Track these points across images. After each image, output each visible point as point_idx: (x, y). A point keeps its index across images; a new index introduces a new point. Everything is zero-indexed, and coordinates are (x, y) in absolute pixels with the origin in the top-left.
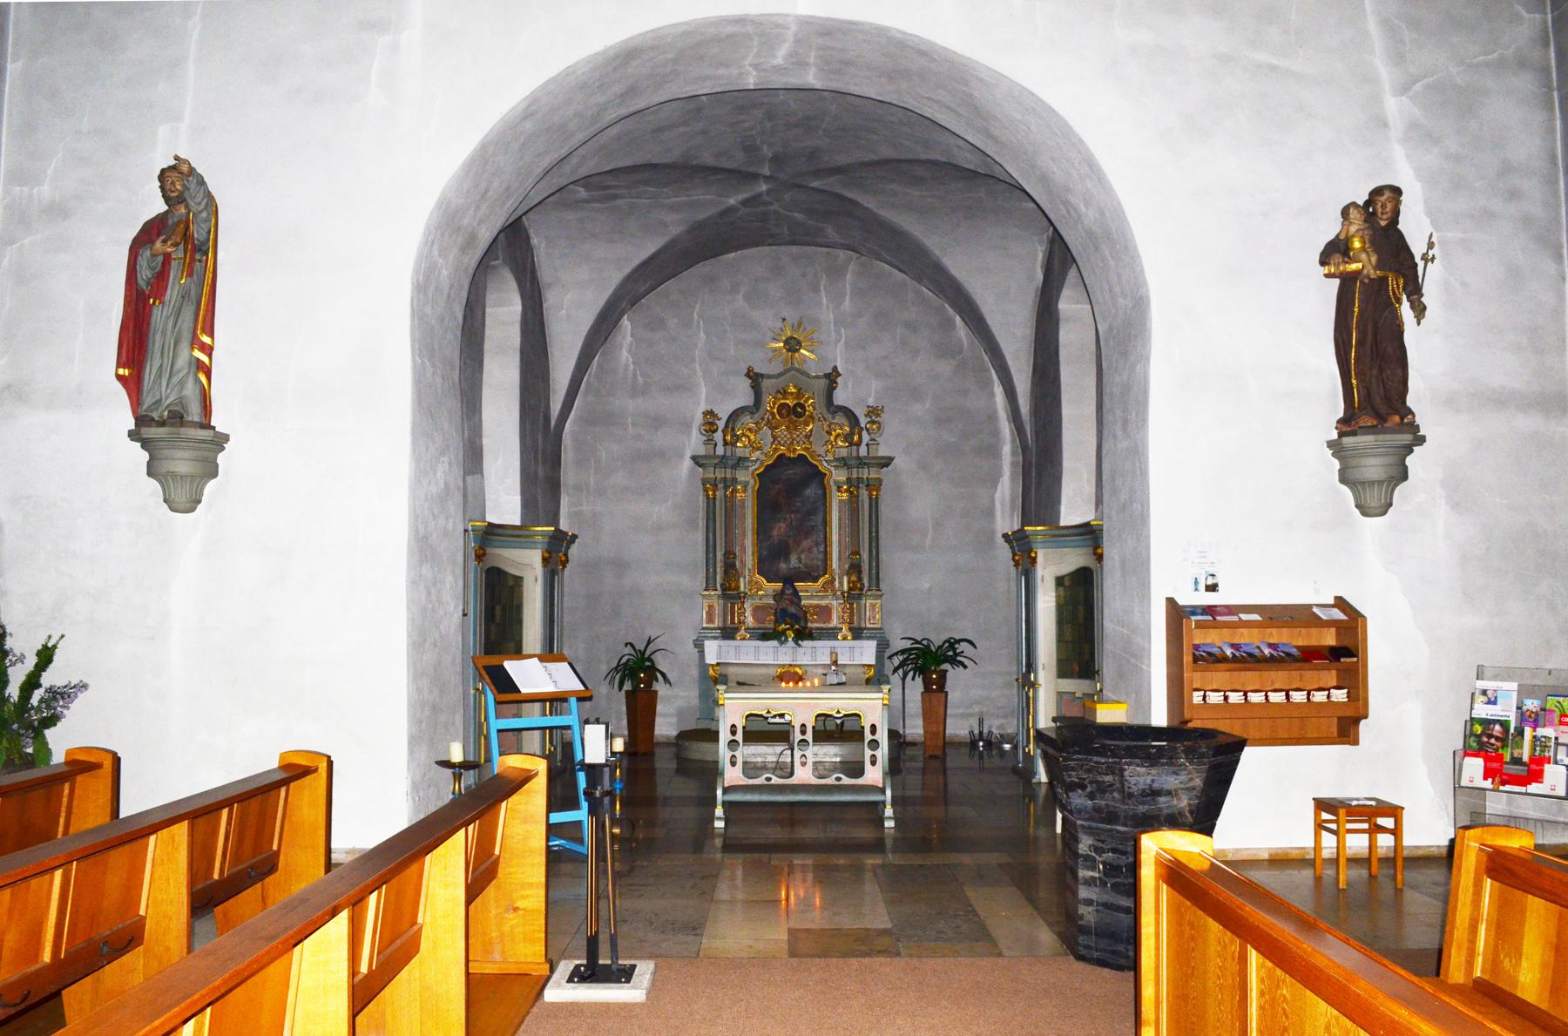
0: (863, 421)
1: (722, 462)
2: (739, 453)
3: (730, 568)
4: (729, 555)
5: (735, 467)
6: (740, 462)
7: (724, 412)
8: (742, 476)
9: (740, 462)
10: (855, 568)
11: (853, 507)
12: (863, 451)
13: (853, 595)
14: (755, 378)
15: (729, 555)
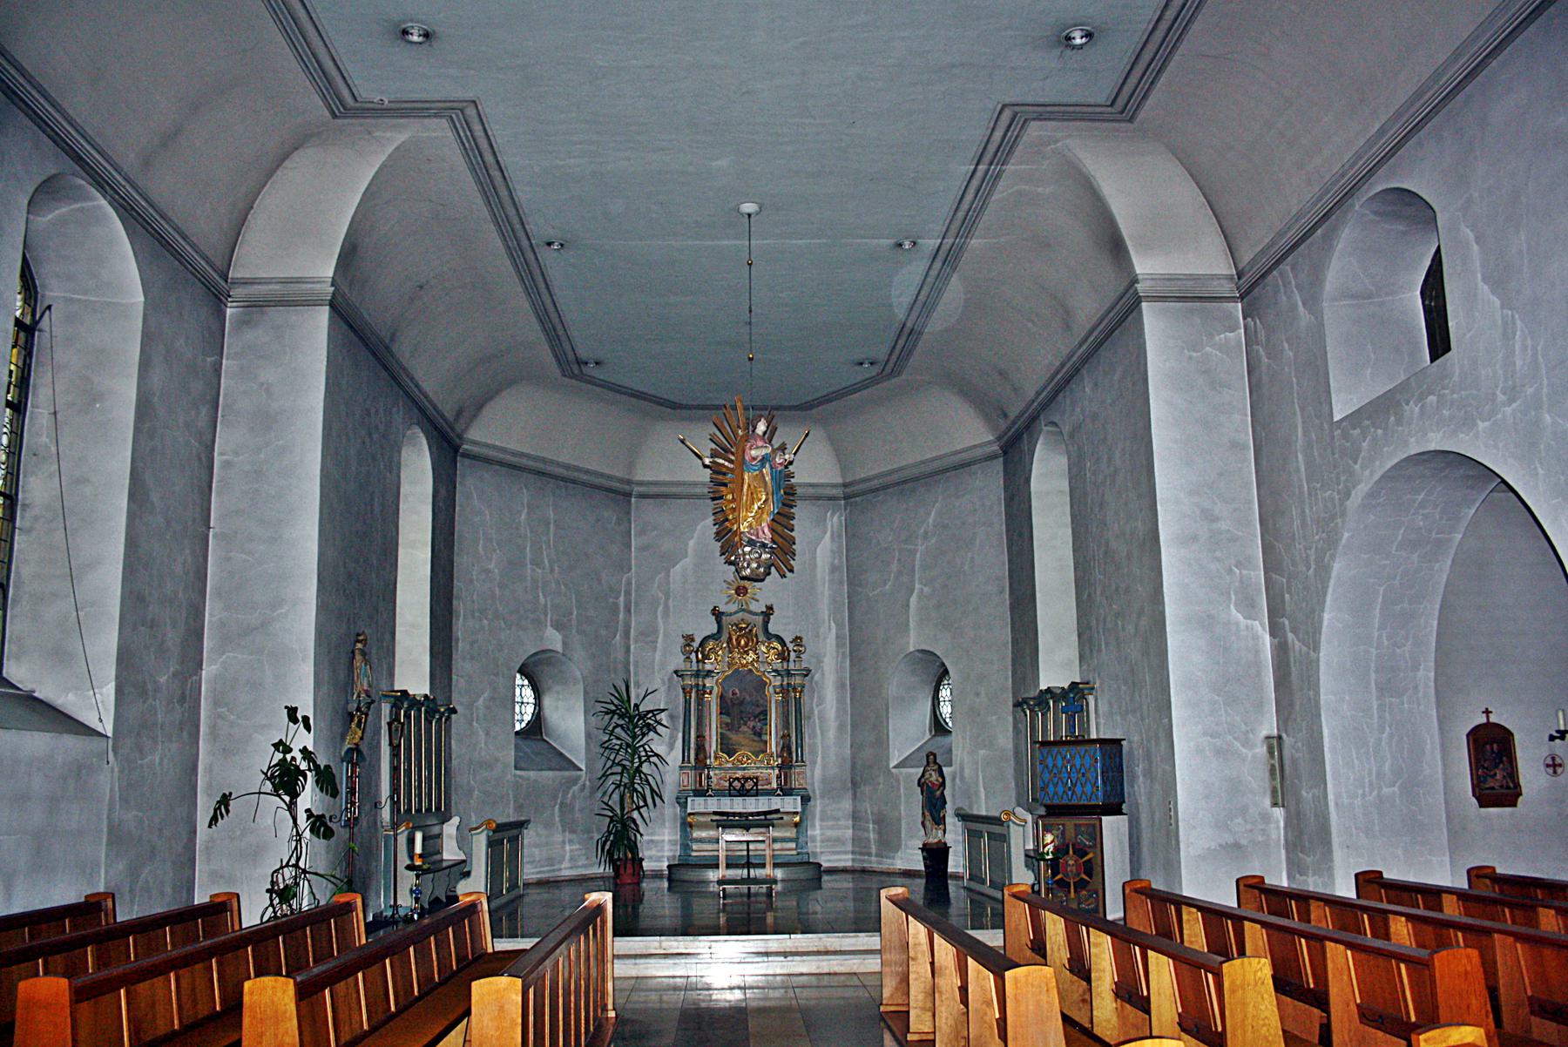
0: (791, 646)
1: (697, 674)
2: (708, 667)
3: (700, 748)
4: (700, 737)
5: (704, 677)
6: (709, 673)
7: (698, 641)
8: (709, 682)
9: (709, 673)
10: (786, 748)
11: (785, 703)
12: (792, 666)
13: (786, 766)
14: (718, 614)
15: (700, 737)
